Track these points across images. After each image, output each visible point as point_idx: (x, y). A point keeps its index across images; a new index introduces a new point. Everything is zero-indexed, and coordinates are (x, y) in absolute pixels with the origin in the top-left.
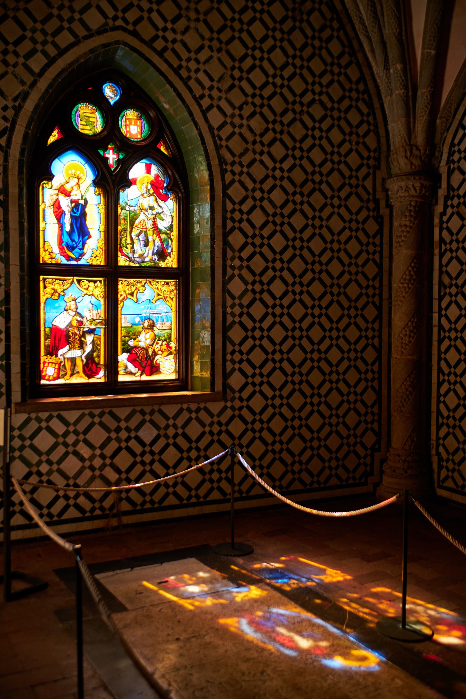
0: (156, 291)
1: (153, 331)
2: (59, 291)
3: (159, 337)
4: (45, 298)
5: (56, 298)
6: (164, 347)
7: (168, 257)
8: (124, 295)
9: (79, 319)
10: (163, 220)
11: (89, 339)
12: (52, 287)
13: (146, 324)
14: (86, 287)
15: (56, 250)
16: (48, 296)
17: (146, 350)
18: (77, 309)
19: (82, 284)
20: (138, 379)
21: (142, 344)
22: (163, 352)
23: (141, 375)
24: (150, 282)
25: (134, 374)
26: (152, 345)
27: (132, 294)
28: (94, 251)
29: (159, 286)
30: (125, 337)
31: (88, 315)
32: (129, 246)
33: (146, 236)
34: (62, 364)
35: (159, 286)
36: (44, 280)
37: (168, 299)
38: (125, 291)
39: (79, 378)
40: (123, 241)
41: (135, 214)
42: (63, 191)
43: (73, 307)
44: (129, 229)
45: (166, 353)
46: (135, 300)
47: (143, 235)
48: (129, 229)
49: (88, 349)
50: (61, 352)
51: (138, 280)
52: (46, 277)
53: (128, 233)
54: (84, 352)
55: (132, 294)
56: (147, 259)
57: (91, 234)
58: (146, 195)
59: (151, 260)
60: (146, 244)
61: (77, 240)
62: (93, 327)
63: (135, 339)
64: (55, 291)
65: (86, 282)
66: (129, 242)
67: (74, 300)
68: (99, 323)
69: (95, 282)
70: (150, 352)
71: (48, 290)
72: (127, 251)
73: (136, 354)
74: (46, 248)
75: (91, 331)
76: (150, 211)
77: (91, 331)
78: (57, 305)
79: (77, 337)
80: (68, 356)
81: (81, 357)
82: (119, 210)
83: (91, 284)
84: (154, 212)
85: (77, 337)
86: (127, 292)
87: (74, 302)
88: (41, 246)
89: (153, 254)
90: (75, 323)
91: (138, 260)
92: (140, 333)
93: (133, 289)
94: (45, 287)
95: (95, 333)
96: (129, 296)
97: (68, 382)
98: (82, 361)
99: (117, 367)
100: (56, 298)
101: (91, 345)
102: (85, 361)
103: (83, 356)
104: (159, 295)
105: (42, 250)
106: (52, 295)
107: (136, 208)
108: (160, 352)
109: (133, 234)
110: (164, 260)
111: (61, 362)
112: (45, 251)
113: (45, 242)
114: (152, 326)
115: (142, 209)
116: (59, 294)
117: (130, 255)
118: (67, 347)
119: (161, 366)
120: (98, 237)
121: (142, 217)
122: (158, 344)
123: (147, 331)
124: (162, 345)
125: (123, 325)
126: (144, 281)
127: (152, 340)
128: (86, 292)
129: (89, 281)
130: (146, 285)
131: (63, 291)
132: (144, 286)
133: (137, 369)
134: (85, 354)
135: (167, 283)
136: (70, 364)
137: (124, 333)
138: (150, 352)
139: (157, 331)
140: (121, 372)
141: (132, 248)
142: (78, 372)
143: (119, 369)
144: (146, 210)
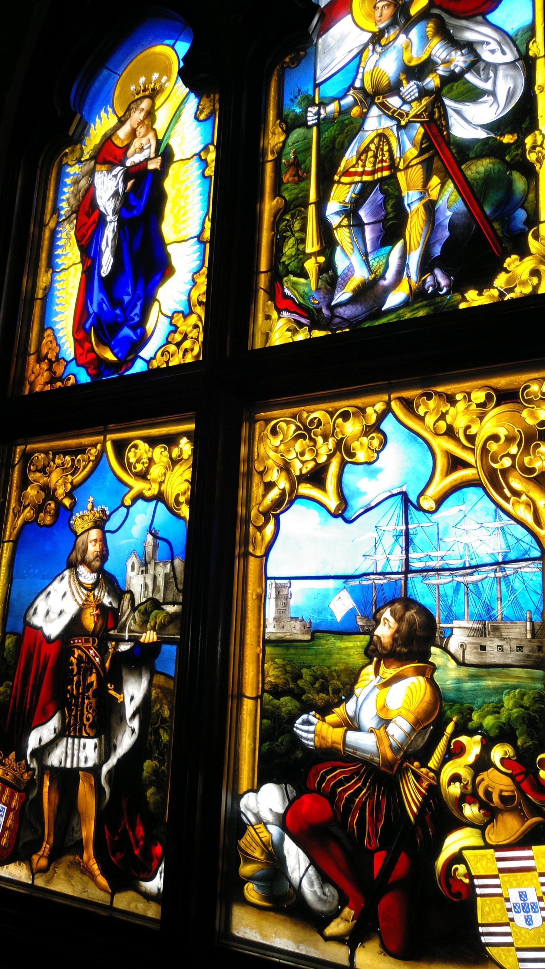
0: (442, 444)
1: (428, 671)
2: (60, 491)
3: (466, 715)
4: (20, 522)
5: (48, 520)
6: (498, 782)
7: (511, 262)
8: (283, 483)
9: (107, 600)
10: (474, 95)
11: (134, 692)
12: (44, 480)
13: (385, 631)
14: (139, 467)
15: (68, 350)
16: (28, 513)
17: (383, 776)
18: (104, 555)
19: (131, 456)
20: (338, 954)
21: (364, 741)
22: (485, 806)
23: (353, 940)
24: (409, 405)
25: (313, 921)
26: (424, 755)
27: (317, 477)
28: (179, 320)
29: (459, 416)
30: (277, 692)
31: (137, 583)
32: (310, 266)
33: (390, 188)
34: (35, 792)
35: (459, 416)
36: (27, 457)
37: (516, 483)
38: (286, 467)
39: (77, 875)
40: (289, 249)
41: (343, 126)
42: (109, 154)
43: (93, 549)
44: (313, 197)
45: (509, 827)
46: (333, 503)
47: (376, 196)
48: (313, 197)
49: (125, 742)
50: (34, 741)
51: (344, 405)
52: (29, 447)
53: (312, 211)
54: (107, 749)
55: (317, 477)
56: (394, 299)
57: (175, 261)
58: (393, 33)
59: (417, 295)
60: (392, 230)
61: (127, 298)
62: (149, 637)
63: (324, 711)
64: (48, 491)
65: (143, 446)
66: (312, 245)
67: (100, 524)
68: (172, 617)
69: (170, 441)
70: (412, 794)
71: (31, 492)
72: (305, 286)
73: (331, 796)
74: (44, 351)
75: (142, 658)
76: (410, 88)
77: (142, 658)
78: (48, 547)
79: (93, 678)
80: (55, 759)
81: (95, 770)
82: (274, 138)
83: (160, 454)
84: (432, 81)
85: (93, 678)
86: (297, 468)
87: (94, 534)
88: (33, 349)
89: (427, 265)
90: (90, 621)
91: (346, 312)
92: (353, 676)
93: (324, 449)
94: (25, 483)
95: (159, 665)
96: (305, 489)
97: (40, 882)
98: (99, 790)
99: (236, 856)
100: (48, 520)
101: (135, 724)
102: (107, 790)
103: (105, 769)
104: (455, 463)
105: (32, 359)
106: (40, 508)
107: (349, 100)
108: (471, 811)
109: (333, 207)
110: (483, 283)
111: (31, 783)
112: (39, 360)
113: (42, 330)
114: (417, 642)
115: (372, 96)
116: (59, 504)
117: (317, 300)
118: (54, 722)
119: (486, 911)
120: (198, 263)
121: (375, 122)
122: (455, 752)
123: (387, 672)
124: (482, 764)
125: (271, 630)
126: (375, 406)
127: (418, 725)
128: (138, 486)
129: (152, 442)
130: (388, 425)
131: (69, 494)
132: (376, 427)
133: (329, 890)
134: (113, 761)
135: (507, 397)
136: (55, 797)
137: (273, 674)
138: (412, 794)
139: (448, 674)
140: (252, 892)
141: (327, 268)
142: (78, 847)
143: (246, 870)
144: (394, 89)
